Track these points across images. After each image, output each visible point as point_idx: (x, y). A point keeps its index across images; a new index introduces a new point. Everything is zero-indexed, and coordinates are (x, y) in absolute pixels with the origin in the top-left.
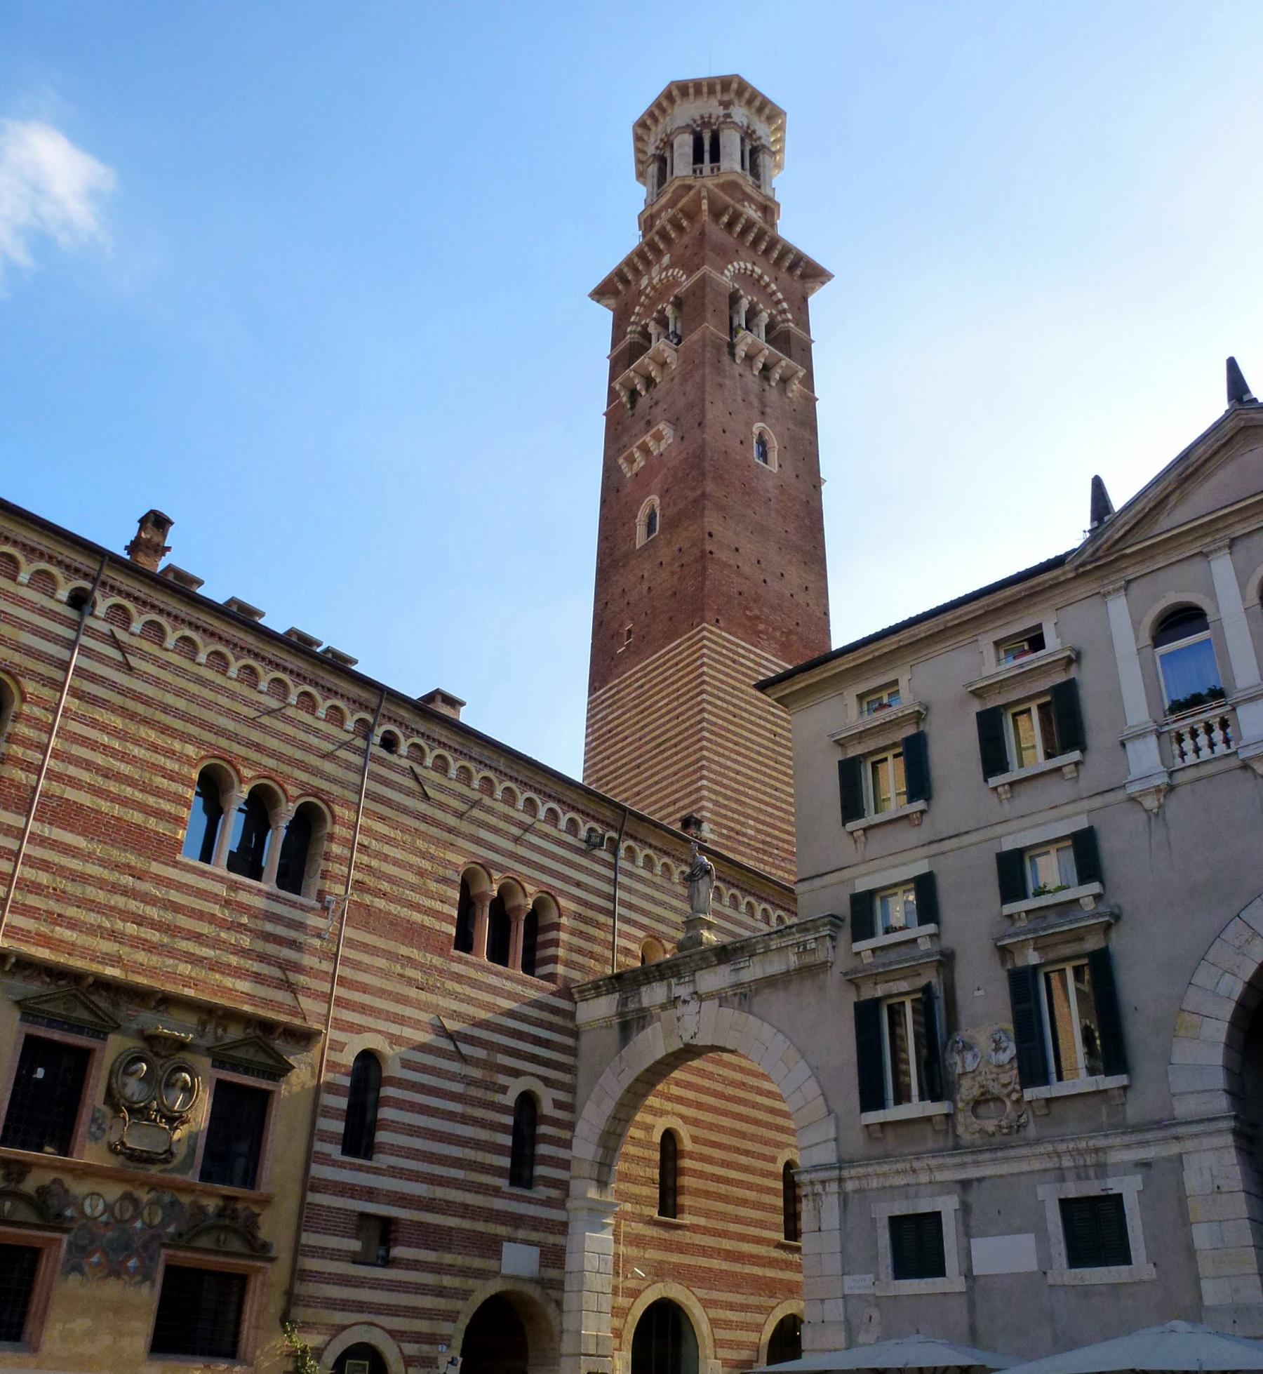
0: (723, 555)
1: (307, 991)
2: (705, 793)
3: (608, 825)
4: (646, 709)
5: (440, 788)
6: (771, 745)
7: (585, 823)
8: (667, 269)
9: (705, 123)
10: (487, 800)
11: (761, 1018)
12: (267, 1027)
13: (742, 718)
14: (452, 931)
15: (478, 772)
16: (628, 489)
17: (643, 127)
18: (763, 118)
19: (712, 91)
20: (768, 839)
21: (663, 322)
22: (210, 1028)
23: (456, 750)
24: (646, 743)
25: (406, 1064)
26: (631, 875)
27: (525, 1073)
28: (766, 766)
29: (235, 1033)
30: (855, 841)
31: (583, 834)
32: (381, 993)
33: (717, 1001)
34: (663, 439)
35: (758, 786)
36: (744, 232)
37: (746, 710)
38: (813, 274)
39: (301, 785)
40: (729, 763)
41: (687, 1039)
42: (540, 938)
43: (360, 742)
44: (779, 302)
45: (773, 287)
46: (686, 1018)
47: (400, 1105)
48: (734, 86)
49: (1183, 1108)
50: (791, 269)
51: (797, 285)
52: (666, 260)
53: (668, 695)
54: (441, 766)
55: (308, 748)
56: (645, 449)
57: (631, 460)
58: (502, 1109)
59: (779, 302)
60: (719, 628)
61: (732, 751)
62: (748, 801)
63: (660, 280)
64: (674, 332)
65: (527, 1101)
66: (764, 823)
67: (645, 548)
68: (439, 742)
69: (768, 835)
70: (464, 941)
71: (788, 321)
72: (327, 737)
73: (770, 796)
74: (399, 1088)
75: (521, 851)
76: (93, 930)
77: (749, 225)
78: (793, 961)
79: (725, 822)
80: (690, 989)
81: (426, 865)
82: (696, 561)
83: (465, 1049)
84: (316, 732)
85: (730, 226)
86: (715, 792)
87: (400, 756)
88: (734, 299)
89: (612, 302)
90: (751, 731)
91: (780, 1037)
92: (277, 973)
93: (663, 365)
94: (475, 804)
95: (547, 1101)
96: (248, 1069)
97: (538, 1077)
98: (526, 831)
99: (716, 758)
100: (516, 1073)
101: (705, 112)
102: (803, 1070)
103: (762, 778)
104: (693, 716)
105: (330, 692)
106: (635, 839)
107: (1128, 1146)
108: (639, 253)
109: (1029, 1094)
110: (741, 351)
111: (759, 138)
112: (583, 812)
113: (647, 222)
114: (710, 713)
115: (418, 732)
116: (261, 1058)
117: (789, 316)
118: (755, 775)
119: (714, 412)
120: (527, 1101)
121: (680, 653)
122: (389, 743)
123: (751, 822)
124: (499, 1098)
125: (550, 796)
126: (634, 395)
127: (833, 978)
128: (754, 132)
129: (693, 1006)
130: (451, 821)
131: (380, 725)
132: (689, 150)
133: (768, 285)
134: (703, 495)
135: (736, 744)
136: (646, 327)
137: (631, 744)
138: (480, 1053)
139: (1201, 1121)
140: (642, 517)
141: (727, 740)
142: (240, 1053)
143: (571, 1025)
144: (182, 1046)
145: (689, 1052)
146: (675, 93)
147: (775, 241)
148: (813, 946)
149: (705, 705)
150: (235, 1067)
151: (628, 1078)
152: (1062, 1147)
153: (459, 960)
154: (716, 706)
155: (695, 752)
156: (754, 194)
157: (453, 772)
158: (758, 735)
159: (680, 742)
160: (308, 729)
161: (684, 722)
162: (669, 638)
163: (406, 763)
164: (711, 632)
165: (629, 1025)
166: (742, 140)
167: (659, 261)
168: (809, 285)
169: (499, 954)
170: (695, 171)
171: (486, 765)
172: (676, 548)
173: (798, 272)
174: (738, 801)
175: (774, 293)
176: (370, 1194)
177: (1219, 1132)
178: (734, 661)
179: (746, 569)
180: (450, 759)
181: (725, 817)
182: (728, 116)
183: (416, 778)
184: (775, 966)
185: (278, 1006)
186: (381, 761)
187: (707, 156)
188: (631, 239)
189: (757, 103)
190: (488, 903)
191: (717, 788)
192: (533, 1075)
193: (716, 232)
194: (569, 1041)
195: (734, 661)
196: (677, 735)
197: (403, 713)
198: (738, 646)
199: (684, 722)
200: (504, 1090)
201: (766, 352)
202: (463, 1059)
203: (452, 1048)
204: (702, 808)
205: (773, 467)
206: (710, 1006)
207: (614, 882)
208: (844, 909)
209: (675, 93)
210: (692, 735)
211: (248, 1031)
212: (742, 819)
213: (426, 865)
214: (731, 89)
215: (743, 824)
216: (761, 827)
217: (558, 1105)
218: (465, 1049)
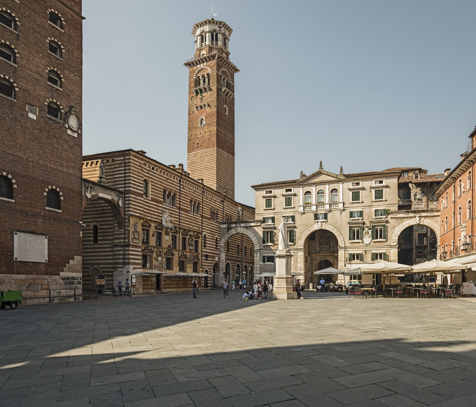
9: (214, 31)
12: (198, 233)
19: (217, 23)
25: (208, 236)
55: (198, 195)
65: (217, 238)
76: (188, 224)
100: (216, 235)
101: (215, 28)
102: (255, 238)
120: (217, 238)
129: (239, 228)
132: (210, 37)
151: (229, 236)
165: (229, 229)
176: (206, 252)
185: (197, 230)
187: (214, 39)
206: (242, 228)
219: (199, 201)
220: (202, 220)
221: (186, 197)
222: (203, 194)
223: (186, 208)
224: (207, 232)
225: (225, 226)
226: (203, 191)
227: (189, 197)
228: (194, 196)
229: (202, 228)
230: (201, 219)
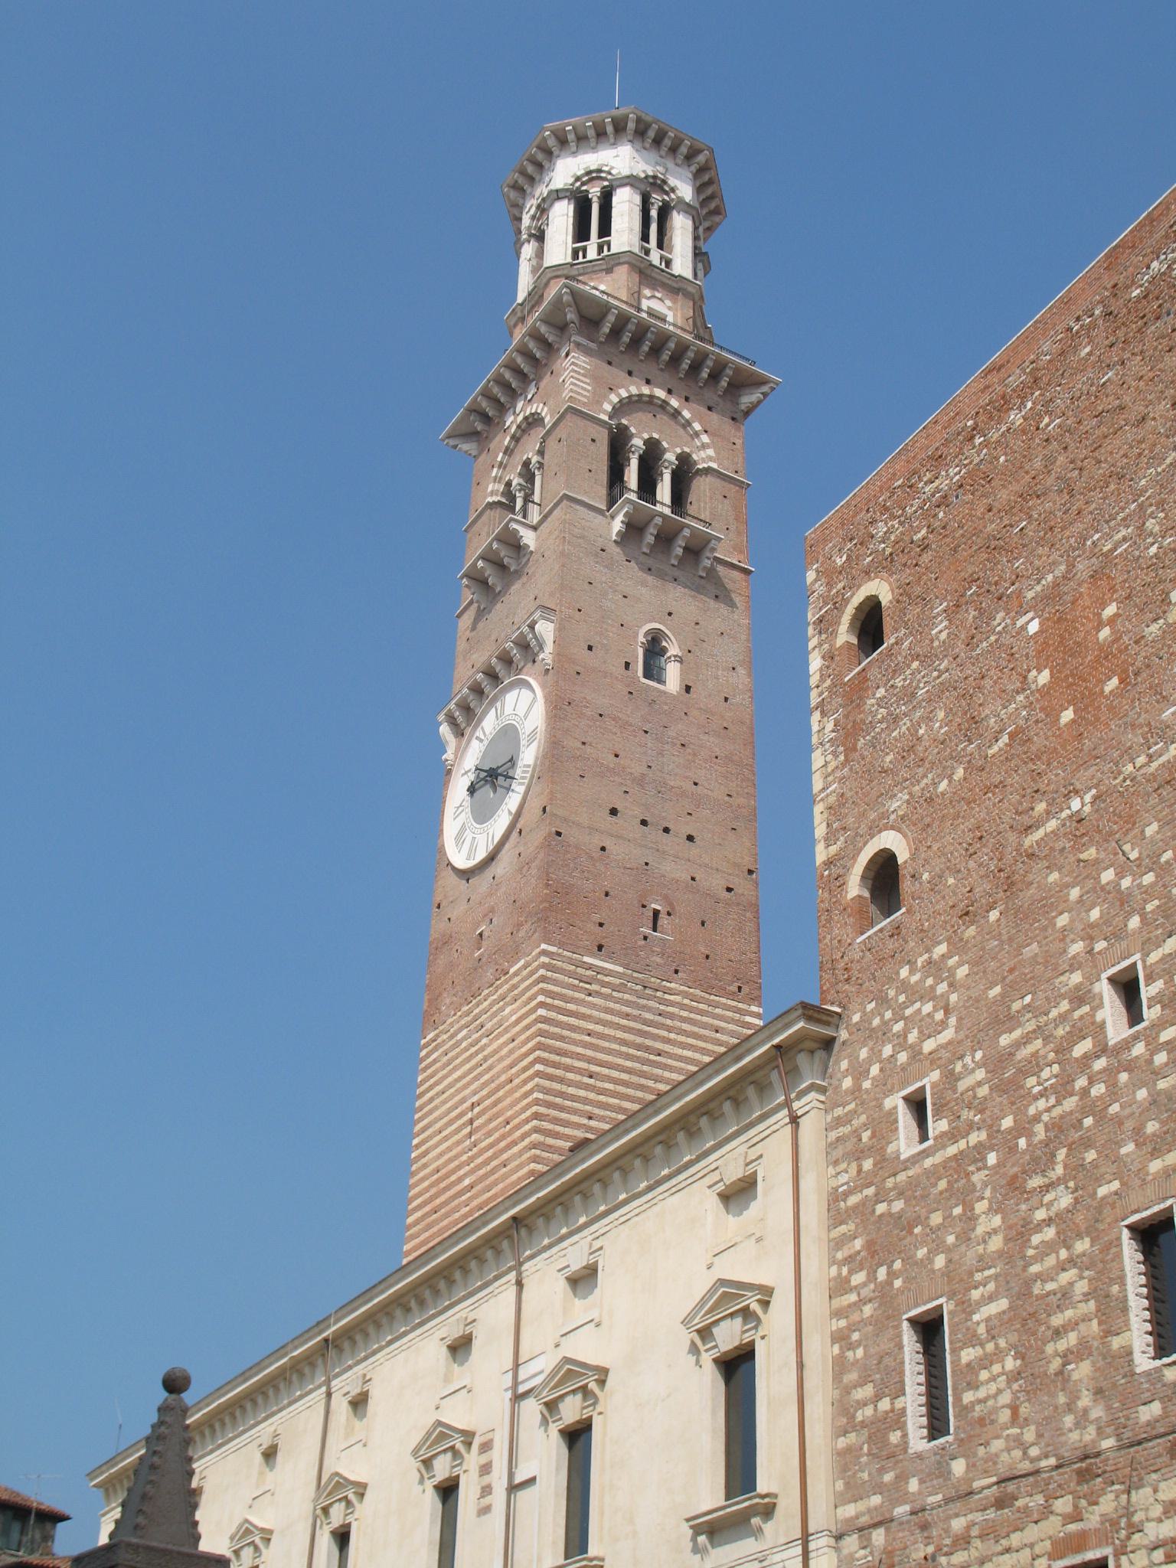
9: (593, 175)
18: (680, 158)
44: (697, 434)
45: (686, 414)
50: (715, 377)
59: (697, 434)
63: (526, 418)
71: (710, 459)
111: (673, 190)
117: (710, 452)
128: (664, 182)
136: (509, 484)
167: (525, 391)
168: (747, 399)
170: (575, 253)
173: (724, 383)
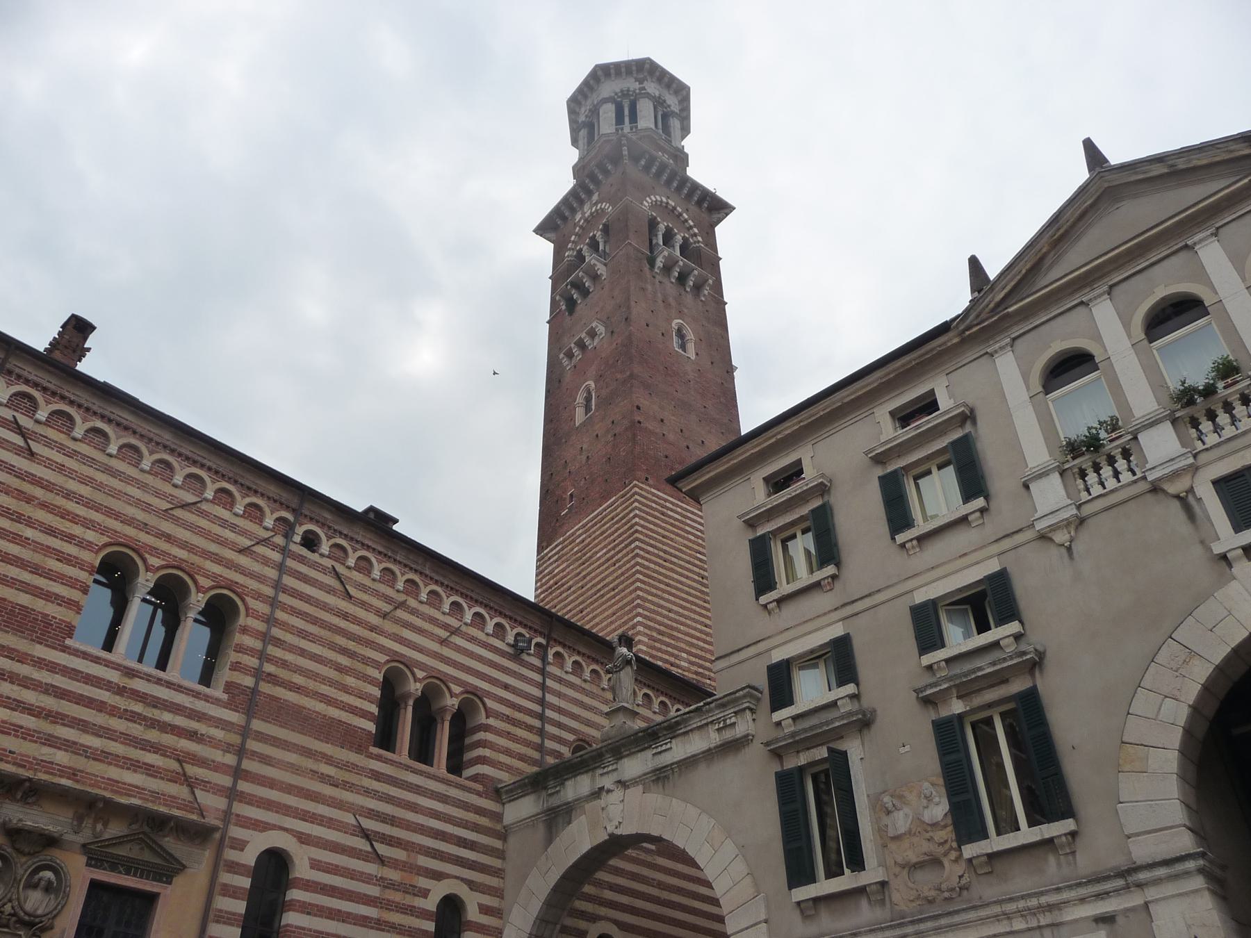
0: (651, 425)
1: (206, 785)
2: (640, 628)
3: (536, 631)
4: (586, 561)
5: (363, 588)
6: (699, 586)
7: (512, 629)
8: (596, 204)
9: (625, 94)
10: (412, 603)
11: (684, 800)
12: (159, 823)
13: (672, 563)
14: (371, 727)
15: (403, 575)
16: (568, 377)
17: (574, 103)
20: (701, 670)
21: (594, 245)
22: (88, 823)
23: (380, 553)
24: (588, 590)
25: (316, 865)
26: (560, 680)
27: (448, 876)
28: (696, 605)
29: (115, 829)
30: (769, 613)
31: (510, 638)
32: (289, 789)
33: (641, 787)
34: (592, 320)
35: (689, 622)
36: (658, 174)
37: (675, 556)
38: (716, 208)
39: (214, 576)
40: (662, 602)
41: (610, 829)
42: (468, 741)
43: (279, 540)
44: (691, 227)
46: (611, 808)
47: (306, 909)
48: (647, 66)
49: (1143, 850)
51: (705, 215)
52: (595, 197)
53: (605, 547)
54: (364, 565)
55: (223, 542)
56: (581, 345)
57: (570, 355)
58: (424, 914)
59: (691, 227)
60: (650, 486)
61: (664, 591)
62: (680, 635)
64: (604, 251)
65: (451, 905)
66: (696, 656)
67: (583, 424)
68: (363, 544)
69: (701, 666)
70: (385, 738)
72: (243, 533)
73: (701, 631)
74: (306, 890)
75: (447, 652)
77: (663, 167)
78: (714, 738)
79: (660, 654)
80: (614, 777)
81: (344, 661)
82: (626, 429)
83: (382, 849)
84: (233, 528)
85: (647, 168)
86: (649, 628)
87: (322, 555)
88: (653, 224)
89: (553, 235)
90: (682, 575)
91: (704, 817)
92: (173, 765)
93: (595, 277)
94: (402, 605)
95: (473, 904)
96: (130, 867)
97: (463, 880)
98: (452, 633)
99: (650, 598)
100: (438, 876)
102: (729, 848)
103: (693, 616)
104: (628, 561)
105: (249, 490)
106: (564, 646)
107: (1082, 900)
108: (573, 193)
109: (969, 850)
110: (659, 263)
112: (511, 618)
113: (578, 170)
114: (643, 558)
115: (341, 533)
116: (147, 856)
118: (686, 613)
119: (639, 310)
120: (451, 905)
121: (615, 509)
122: (310, 542)
123: (684, 655)
124: (419, 902)
125: (476, 601)
126: (571, 304)
127: (756, 751)
129: (618, 794)
130: (374, 619)
131: (301, 525)
133: (681, 214)
134: (632, 376)
135: (668, 585)
137: (574, 592)
138: (399, 854)
139: (1166, 863)
140: (580, 399)
141: (660, 581)
142: (122, 851)
143: (499, 827)
144: (51, 841)
145: (616, 845)
146: (600, 73)
147: (686, 180)
148: (733, 720)
149: (637, 551)
150: (114, 864)
152: (1011, 907)
153: (379, 758)
154: (648, 552)
155: (631, 593)
156: (667, 147)
157: (376, 573)
158: (687, 577)
159: (617, 586)
160: (224, 523)
161: (620, 568)
162: (605, 498)
163: (328, 563)
164: (641, 489)
165: (556, 818)
166: (655, 108)
168: (716, 216)
169: (422, 752)
171: (411, 569)
172: (609, 422)
174: (671, 636)
175: (686, 221)
177: (1187, 873)
178: (663, 514)
179: (671, 437)
180: (374, 560)
181: (659, 650)
182: (644, 89)
183: (338, 576)
184: (695, 744)
185: (171, 800)
186: (302, 560)
187: (627, 120)
188: (567, 183)
189: (666, 80)
190: (411, 702)
191: (652, 624)
192: (457, 878)
193: (634, 172)
194: (497, 844)
195: (663, 514)
196: (614, 580)
197: (327, 515)
198: (666, 500)
199: (620, 568)
200: (425, 893)
201: (681, 263)
202: (381, 860)
203: (369, 849)
204: (634, 627)
205: (691, 353)
206: (635, 792)
207: (543, 687)
208: (762, 682)
209: (600, 73)
210: (628, 578)
211: (134, 827)
212: (676, 652)
213: (344, 661)
214: (645, 69)
215: (676, 657)
216: (693, 659)
217: (485, 910)
218: (382, 849)
219: (231, 585)
220: (245, 732)
221: (41, 515)
222: (284, 551)
223: (24, 599)
224: (304, 839)
225: (523, 809)
226: (286, 528)
227: (88, 524)
228: (169, 538)
229: (232, 794)
230: (234, 717)
